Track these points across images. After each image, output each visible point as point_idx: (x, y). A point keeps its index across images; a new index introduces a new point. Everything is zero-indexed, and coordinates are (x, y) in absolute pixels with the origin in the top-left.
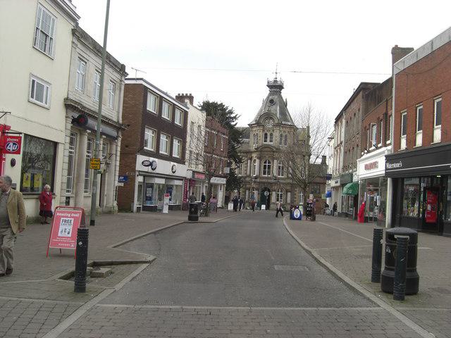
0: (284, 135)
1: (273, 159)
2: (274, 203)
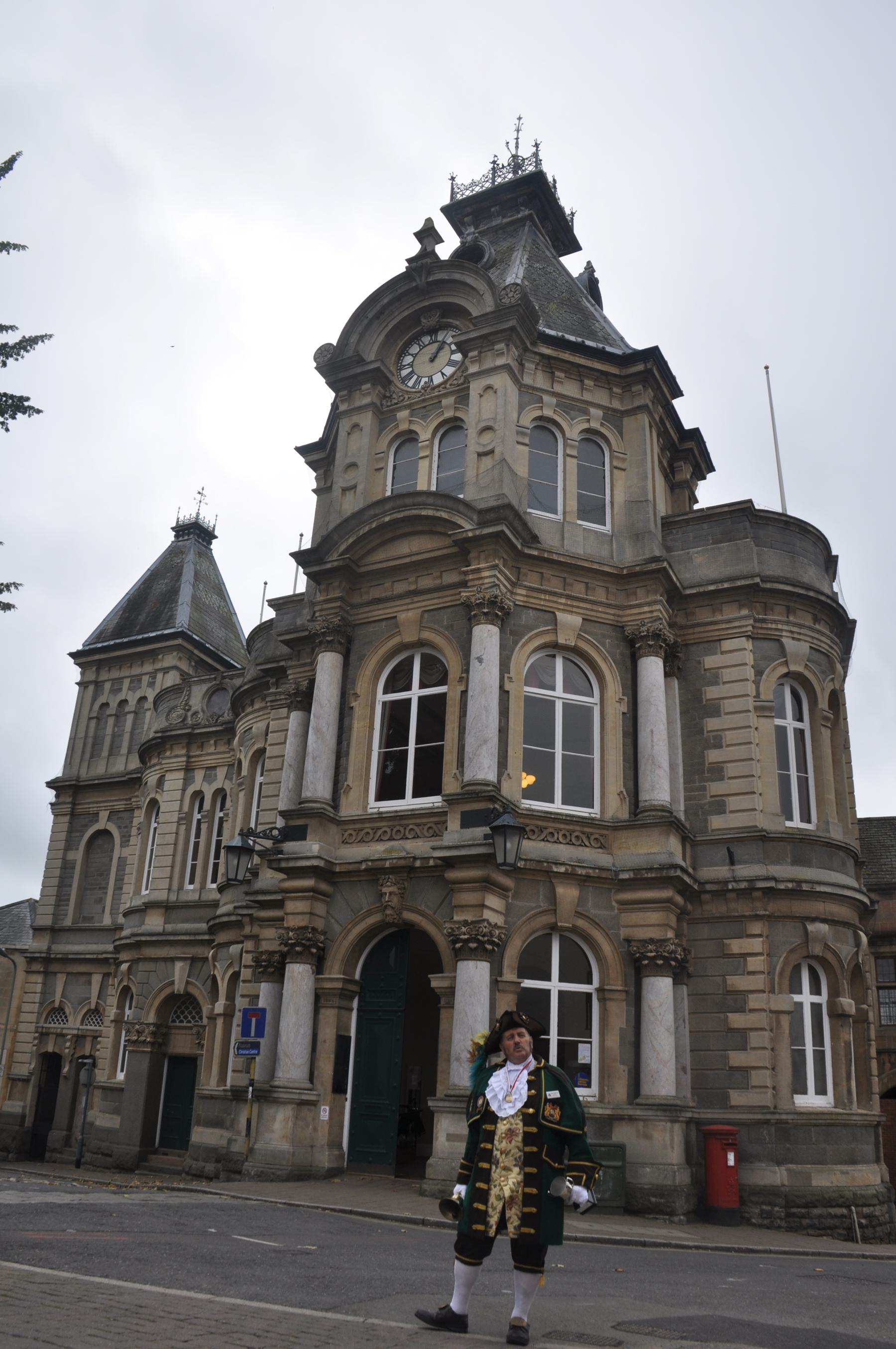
0: (574, 430)
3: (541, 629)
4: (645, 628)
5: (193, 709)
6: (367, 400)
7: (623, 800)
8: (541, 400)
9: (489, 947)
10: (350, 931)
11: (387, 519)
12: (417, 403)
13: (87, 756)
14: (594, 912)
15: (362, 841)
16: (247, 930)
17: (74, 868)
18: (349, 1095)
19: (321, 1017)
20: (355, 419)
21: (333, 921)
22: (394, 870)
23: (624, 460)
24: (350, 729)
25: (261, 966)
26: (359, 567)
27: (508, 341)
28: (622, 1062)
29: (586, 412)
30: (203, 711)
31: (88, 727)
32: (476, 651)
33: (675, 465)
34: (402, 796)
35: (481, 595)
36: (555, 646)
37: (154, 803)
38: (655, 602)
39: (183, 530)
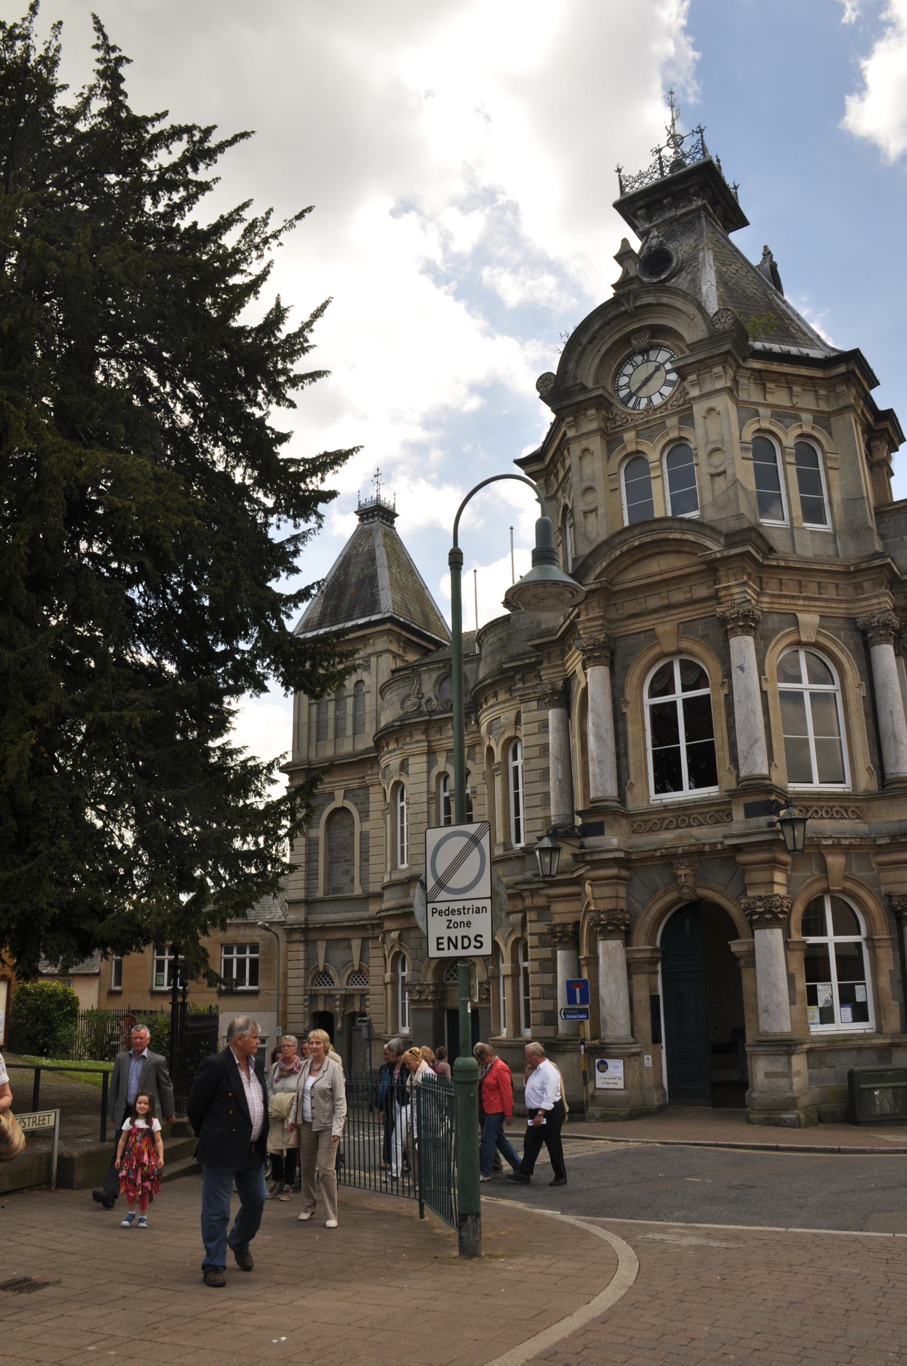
0: (789, 439)
1: (723, 629)
2: (785, 1046)
3: (786, 631)
4: (876, 619)
5: (427, 696)
6: (594, 426)
7: (871, 774)
8: (757, 413)
9: (781, 916)
10: (650, 908)
11: (636, 543)
12: (641, 424)
13: (314, 739)
14: (859, 874)
15: (651, 830)
16: (528, 902)
17: (318, 844)
18: (663, 1044)
19: (634, 982)
20: (585, 443)
21: (633, 900)
22: (686, 855)
23: (836, 459)
24: (625, 732)
25: (556, 937)
26: (613, 586)
27: (724, 364)
28: (894, 999)
29: (797, 418)
30: (437, 698)
31: (309, 712)
32: (735, 660)
33: (872, 445)
34: (679, 787)
35: (736, 610)
36: (799, 643)
37: (398, 785)
38: (882, 595)
39: (367, 514)
